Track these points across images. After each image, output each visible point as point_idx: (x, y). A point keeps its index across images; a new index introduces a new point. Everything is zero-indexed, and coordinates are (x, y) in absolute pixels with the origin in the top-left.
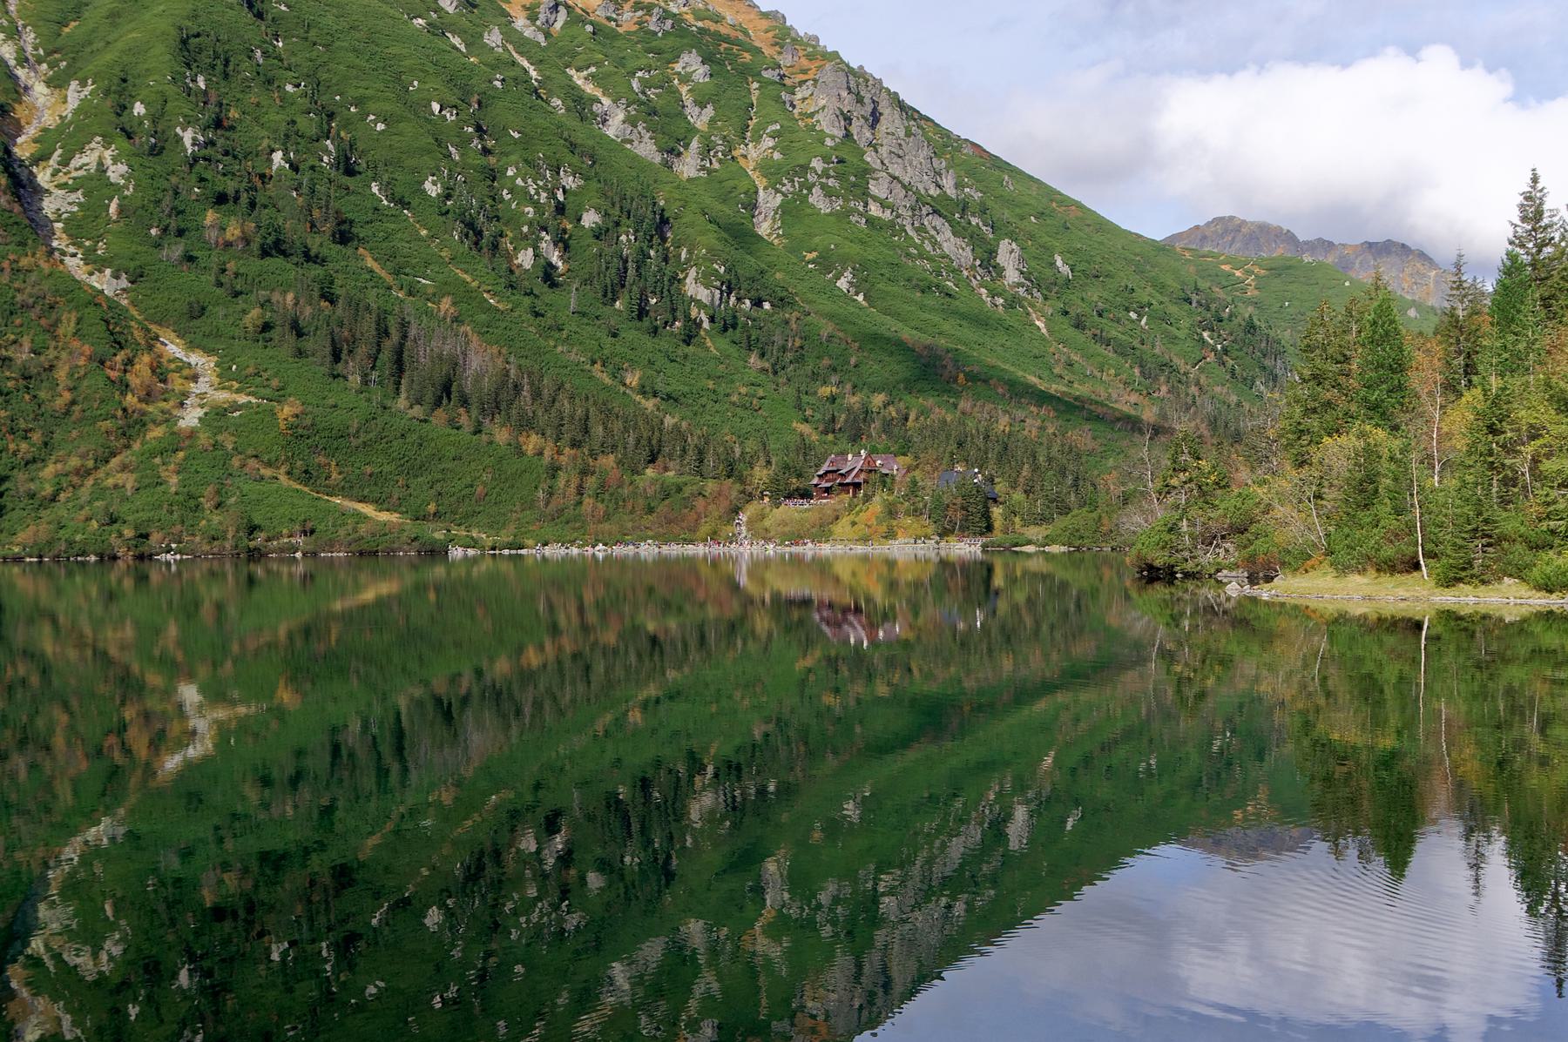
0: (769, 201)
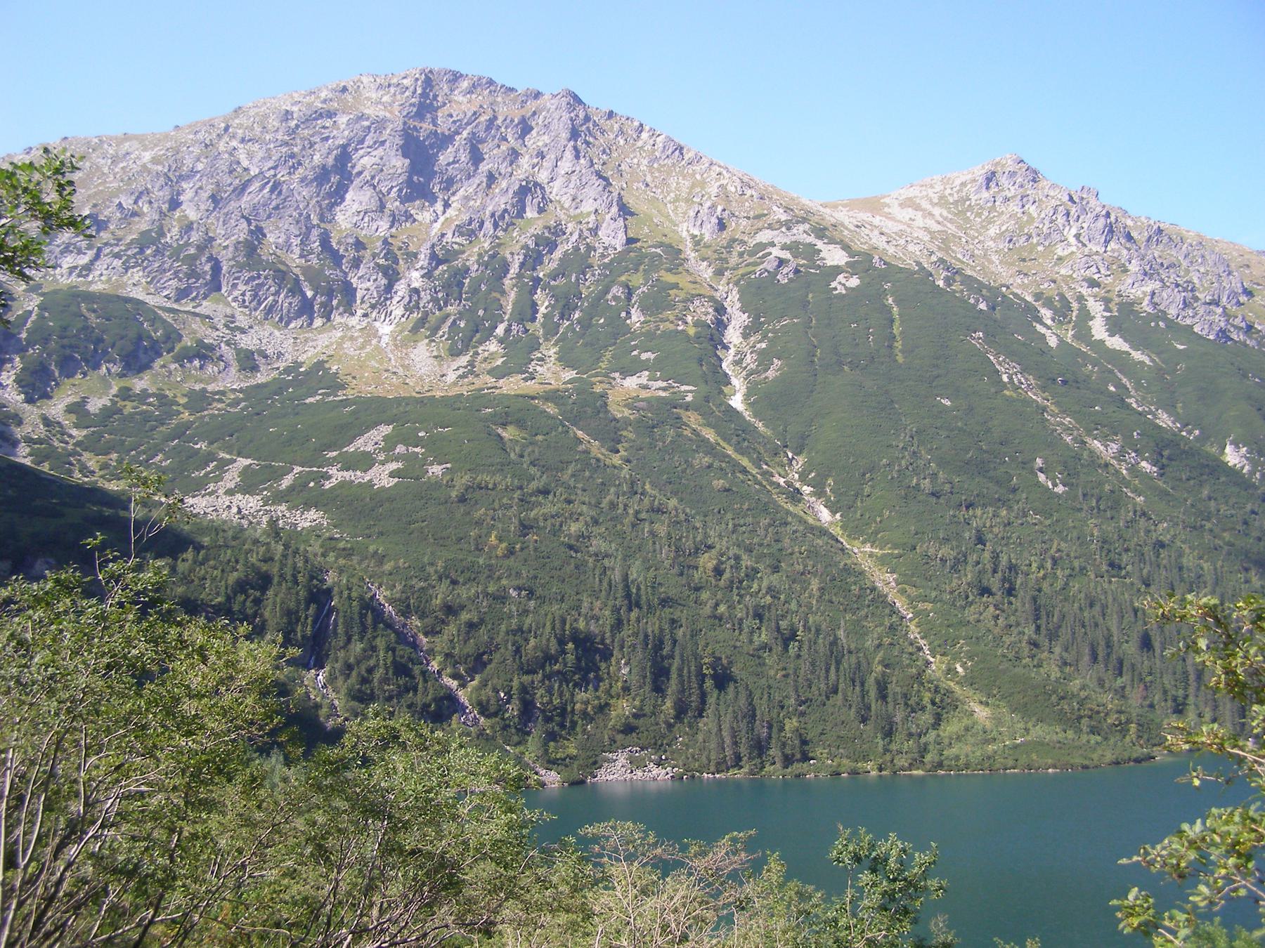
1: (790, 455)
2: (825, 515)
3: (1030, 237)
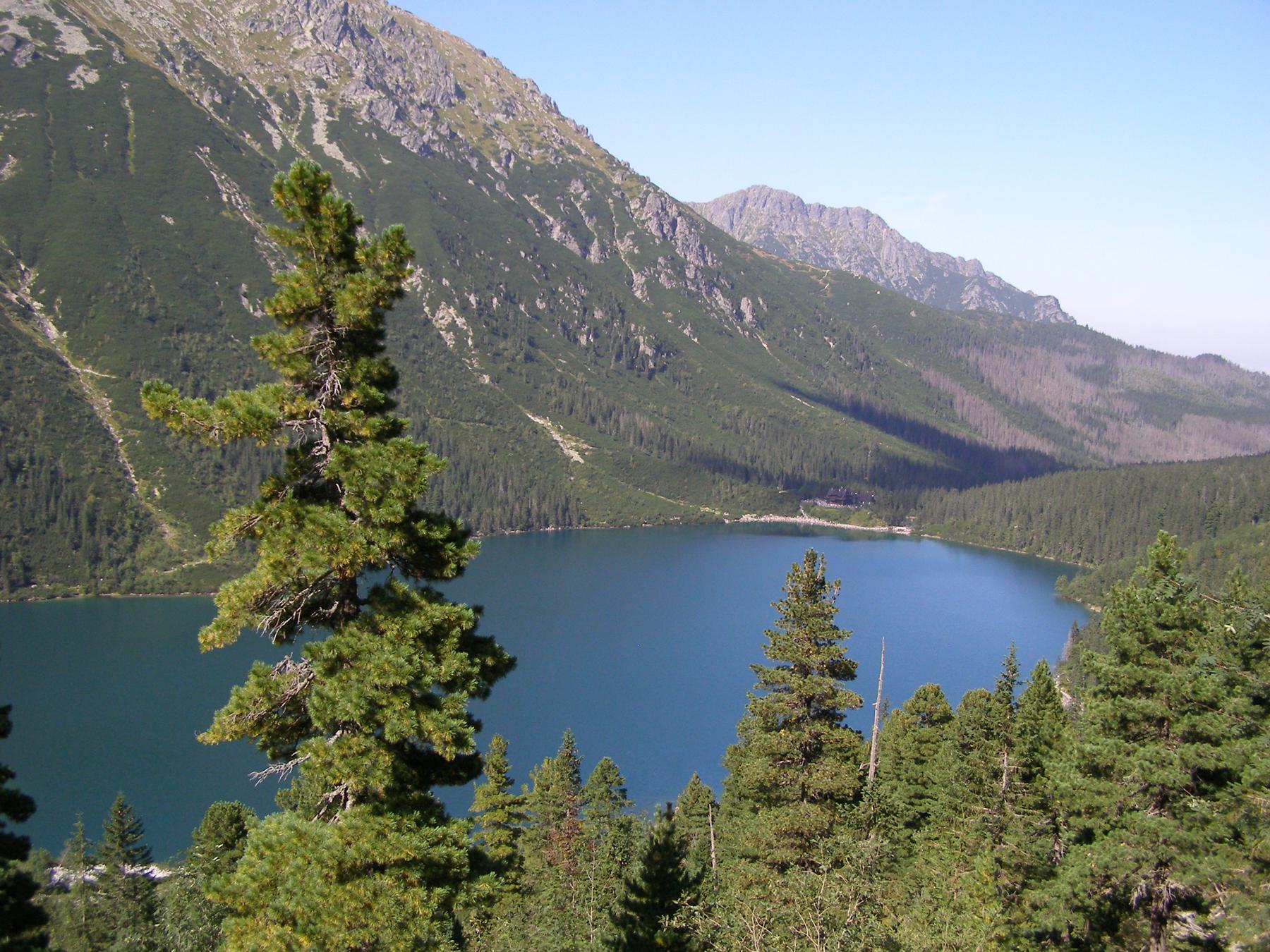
0: (638, 279)
1: (23, 267)
2: (53, 331)
3: (270, 23)
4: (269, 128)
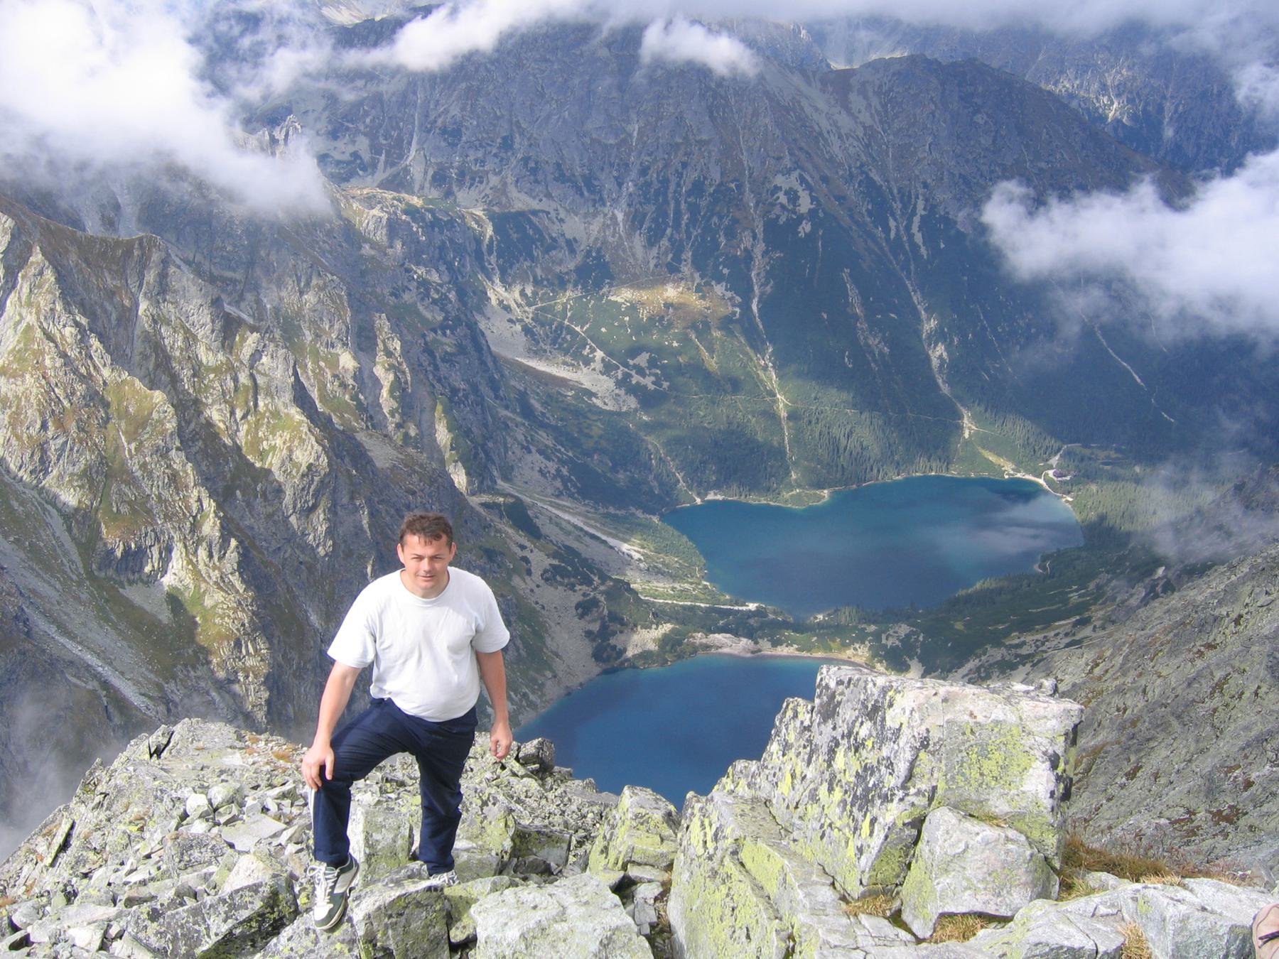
4: (892, 224)
